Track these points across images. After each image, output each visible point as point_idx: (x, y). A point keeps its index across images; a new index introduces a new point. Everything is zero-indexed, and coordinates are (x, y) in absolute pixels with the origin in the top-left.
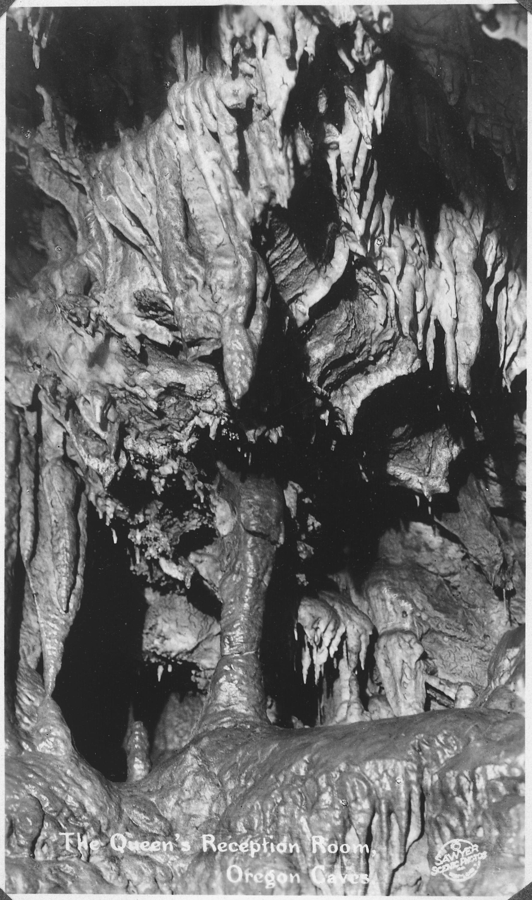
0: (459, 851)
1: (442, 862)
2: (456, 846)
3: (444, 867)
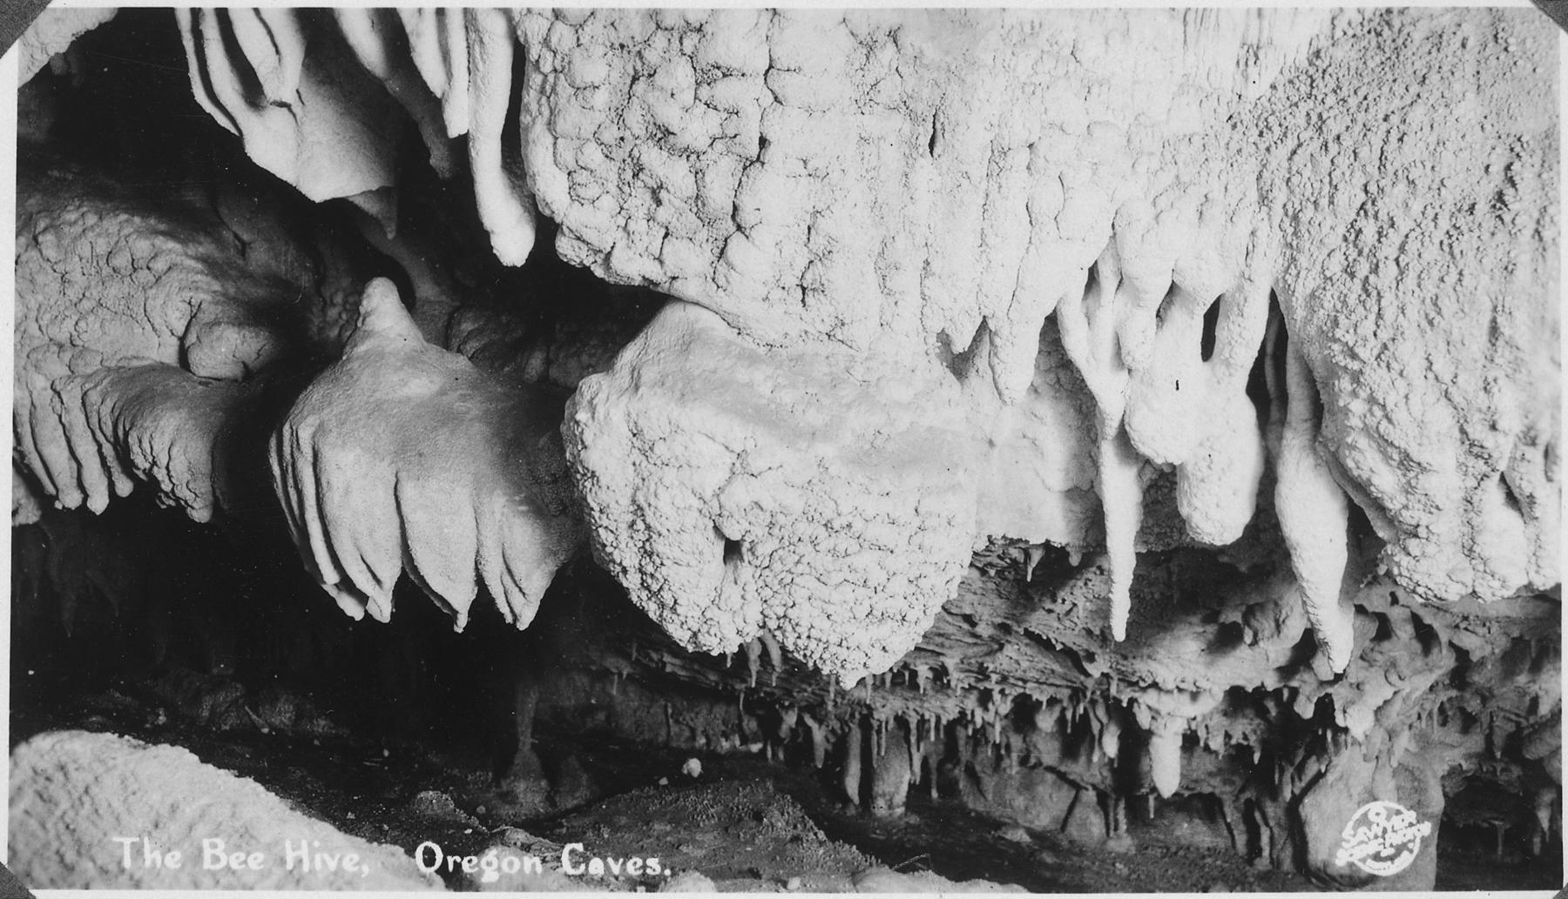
1: (1354, 841)
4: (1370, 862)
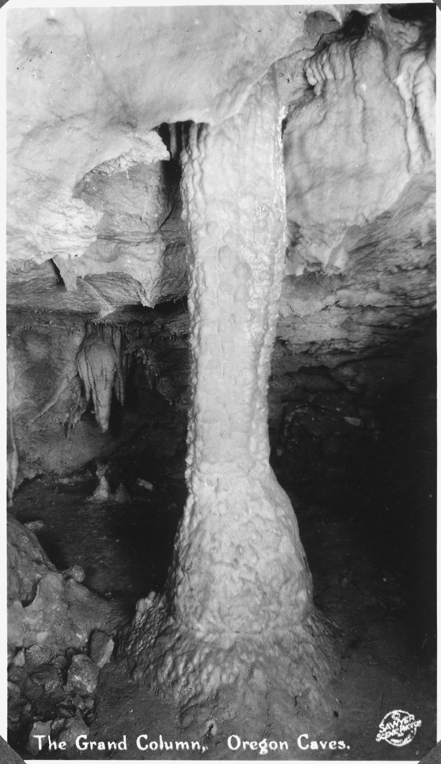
0: (399, 720)
1: (385, 730)
2: (396, 716)
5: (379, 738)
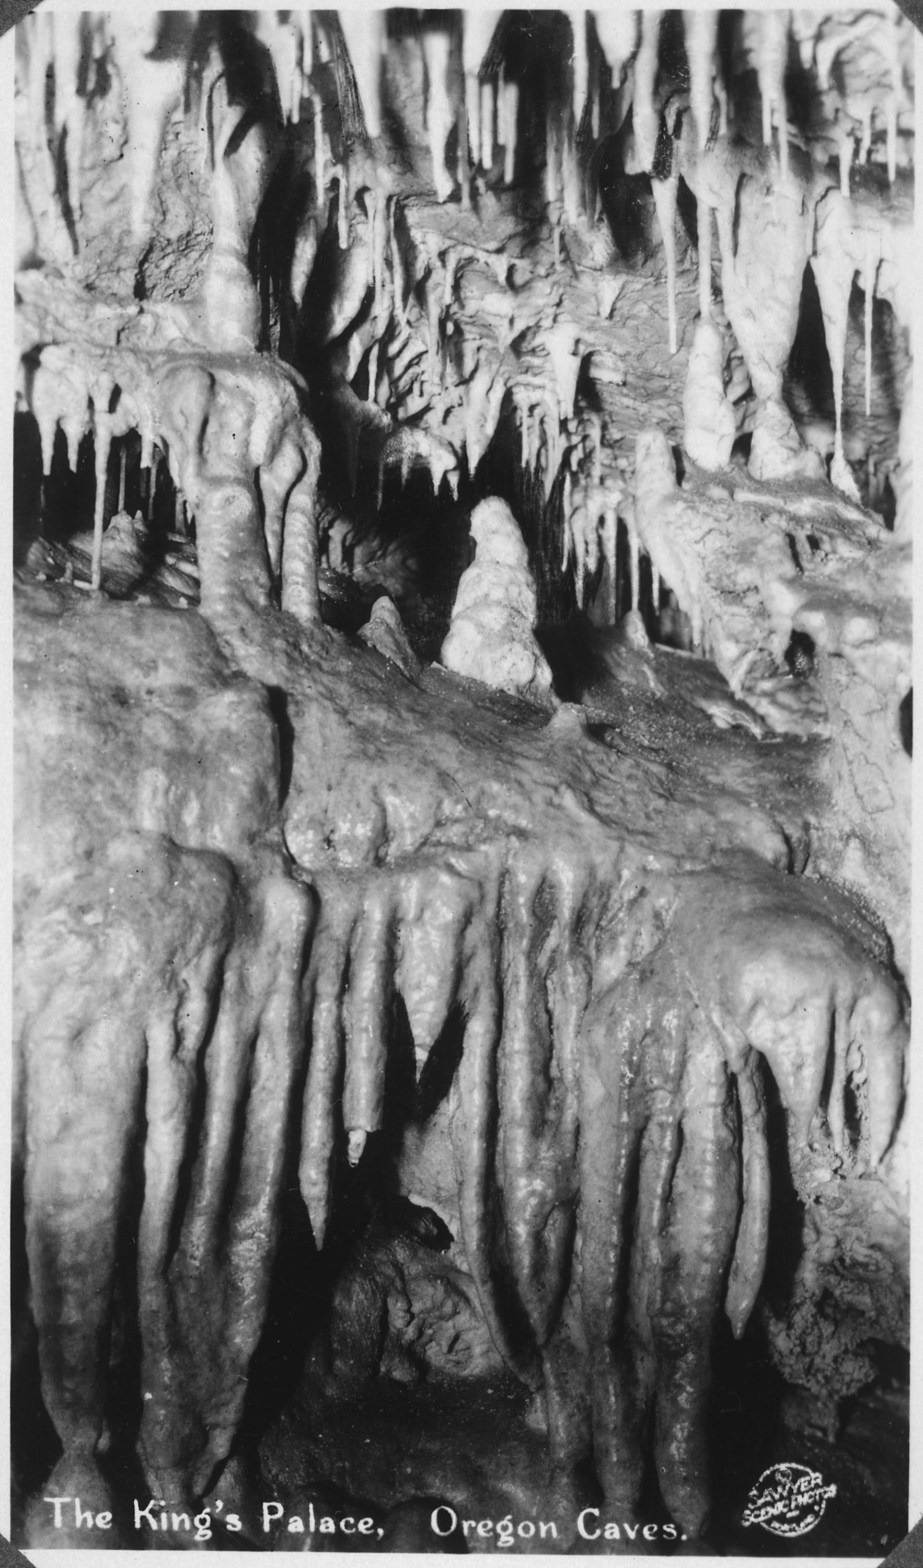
3: (763, 1512)
4: (776, 1524)
5: (750, 1519)
